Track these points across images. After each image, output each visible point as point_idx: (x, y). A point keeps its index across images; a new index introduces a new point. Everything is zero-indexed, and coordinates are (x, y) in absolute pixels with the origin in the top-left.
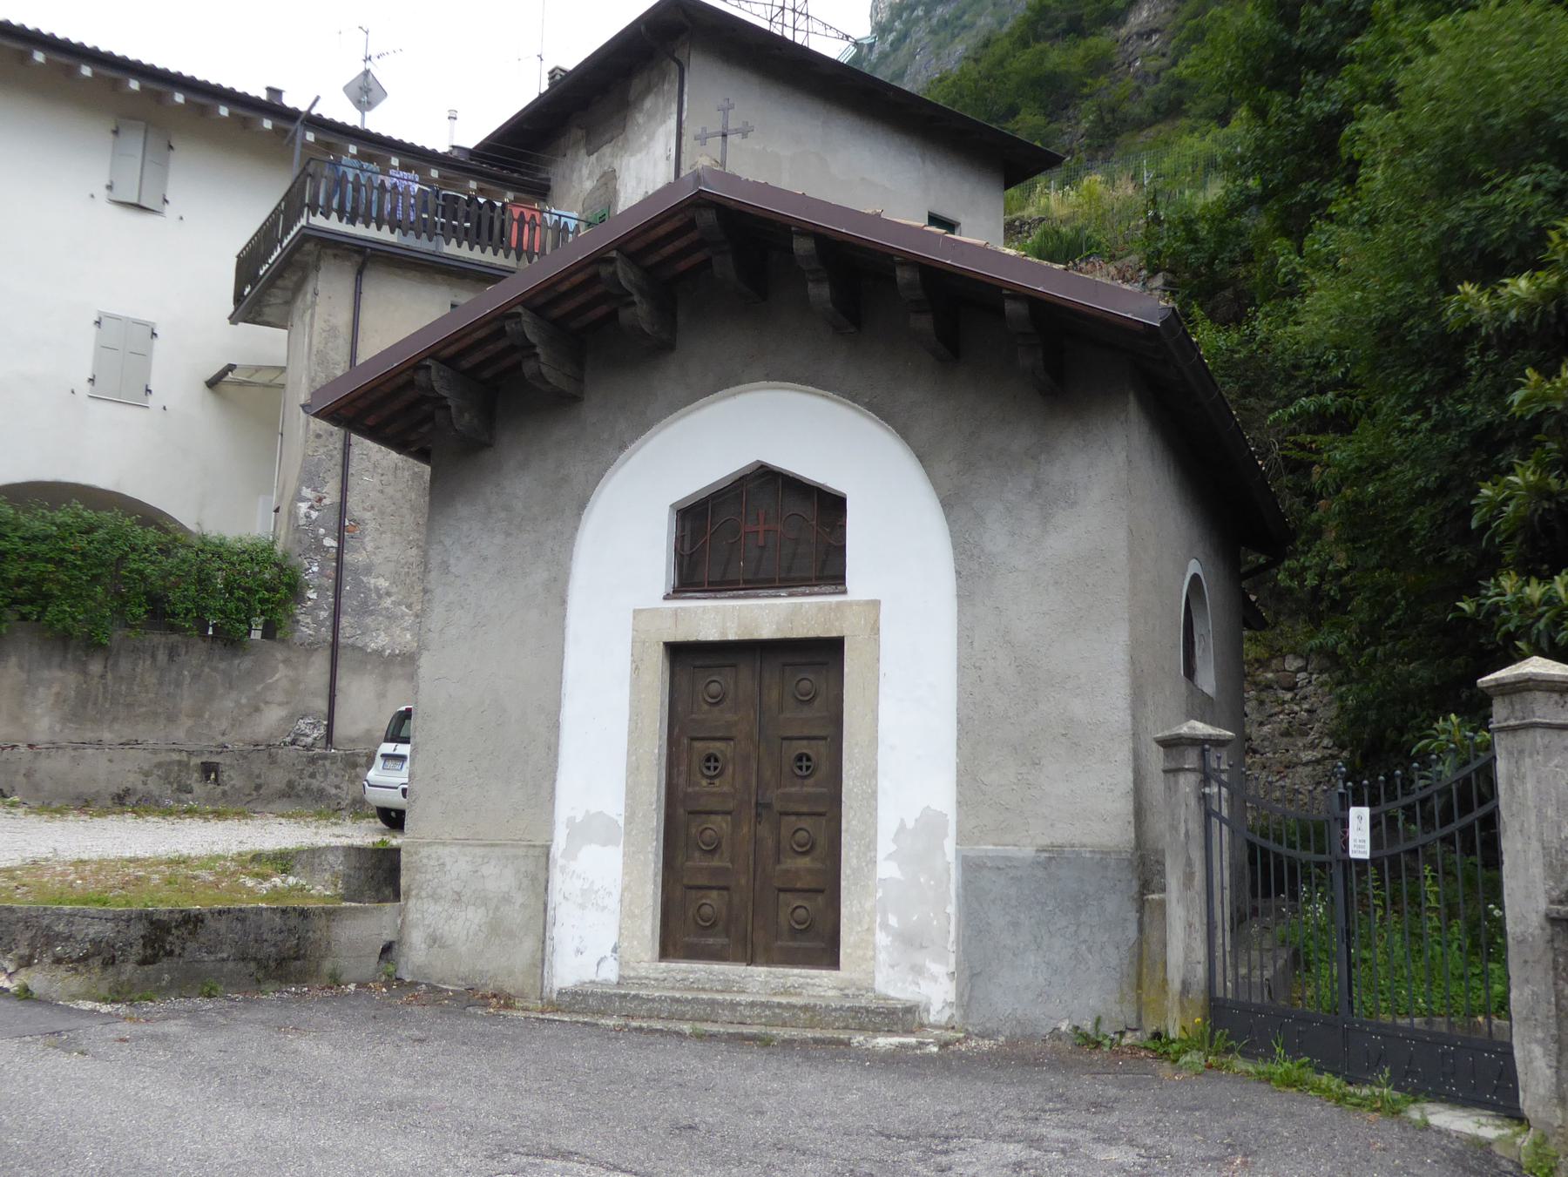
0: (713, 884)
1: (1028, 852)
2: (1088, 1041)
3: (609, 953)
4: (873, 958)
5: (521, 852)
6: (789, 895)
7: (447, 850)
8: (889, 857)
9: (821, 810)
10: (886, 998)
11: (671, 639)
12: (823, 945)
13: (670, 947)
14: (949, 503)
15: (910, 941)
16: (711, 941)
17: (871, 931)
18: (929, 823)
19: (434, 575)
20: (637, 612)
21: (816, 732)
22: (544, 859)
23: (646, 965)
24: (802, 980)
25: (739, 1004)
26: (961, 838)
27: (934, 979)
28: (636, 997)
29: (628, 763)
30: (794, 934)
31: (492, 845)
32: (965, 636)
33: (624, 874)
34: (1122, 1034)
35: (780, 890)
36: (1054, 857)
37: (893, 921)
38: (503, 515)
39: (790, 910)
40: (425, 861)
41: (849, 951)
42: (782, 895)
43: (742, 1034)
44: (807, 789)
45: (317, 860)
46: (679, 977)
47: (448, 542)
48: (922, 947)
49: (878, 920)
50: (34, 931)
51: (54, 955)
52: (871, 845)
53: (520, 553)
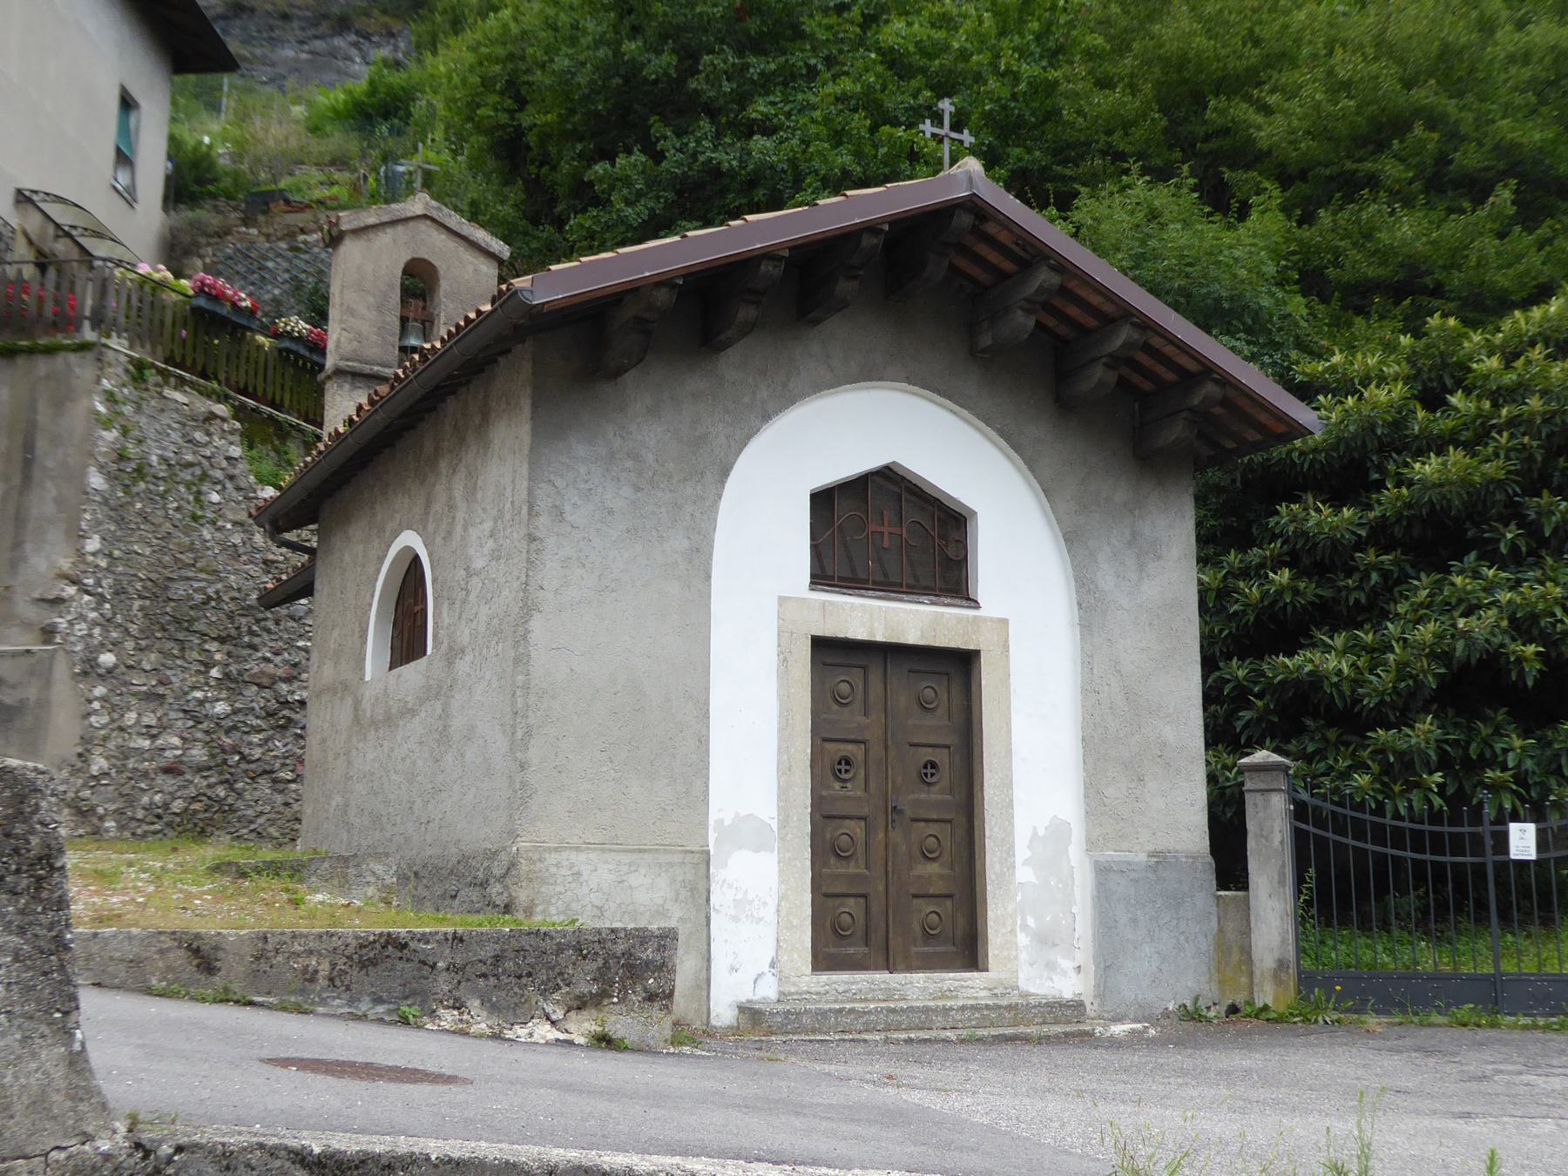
0: (853, 892)
1: (1142, 857)
2: (1192, 1015)
3: (766, 968)
4: (1016, 958)
5: (677, 858)
6: (921, 901)
7: (583, 857)
8: (1026, 862)
9: (947, 817)
10: (1028, 995)
11: (820, 633)
12: (951, 949)
13: (823, 961)
14: (1072, 539)
15: (1045, 940)
16: (851, 950)
17: (1013, 932)
18: (1058, 831)
19: (543, 520)
20: (782, 600)
21: (940, 741)
22: (703, 867)
23: (807, 979)
24: (957, 983)
25: (951, 1009)
26: (1091, 844)
27: (1064, 973)
28: (852, 1011)
29: (779, 762)
30: (928, 937)
31: (640, 851)
32: (1087, 661)
33: (782, 882)
34: (1208, 1008)
35: (915, 896)
36: (1161, 860)
37: (1031, 922)
38: (629, 464)
39: (923, 915)
40: (553, 870)
41: (996, 952)
42: (915, 901)
43: (1004, 1035)
44: (933, 796)
45: (352, 871)
46: (840, 990)
47: (559, 483)
48: (1055, 945)
49: (1019, 922)
50: (600, 962)
51: (645, 990)
52: (1010, 852)
53: (653, 513)
